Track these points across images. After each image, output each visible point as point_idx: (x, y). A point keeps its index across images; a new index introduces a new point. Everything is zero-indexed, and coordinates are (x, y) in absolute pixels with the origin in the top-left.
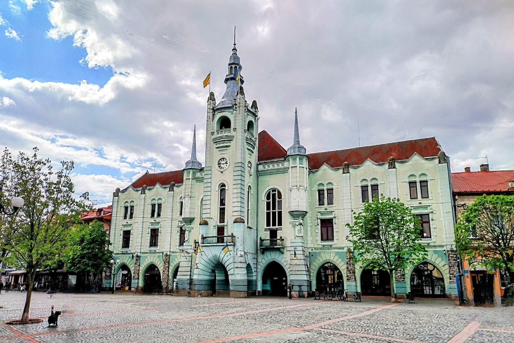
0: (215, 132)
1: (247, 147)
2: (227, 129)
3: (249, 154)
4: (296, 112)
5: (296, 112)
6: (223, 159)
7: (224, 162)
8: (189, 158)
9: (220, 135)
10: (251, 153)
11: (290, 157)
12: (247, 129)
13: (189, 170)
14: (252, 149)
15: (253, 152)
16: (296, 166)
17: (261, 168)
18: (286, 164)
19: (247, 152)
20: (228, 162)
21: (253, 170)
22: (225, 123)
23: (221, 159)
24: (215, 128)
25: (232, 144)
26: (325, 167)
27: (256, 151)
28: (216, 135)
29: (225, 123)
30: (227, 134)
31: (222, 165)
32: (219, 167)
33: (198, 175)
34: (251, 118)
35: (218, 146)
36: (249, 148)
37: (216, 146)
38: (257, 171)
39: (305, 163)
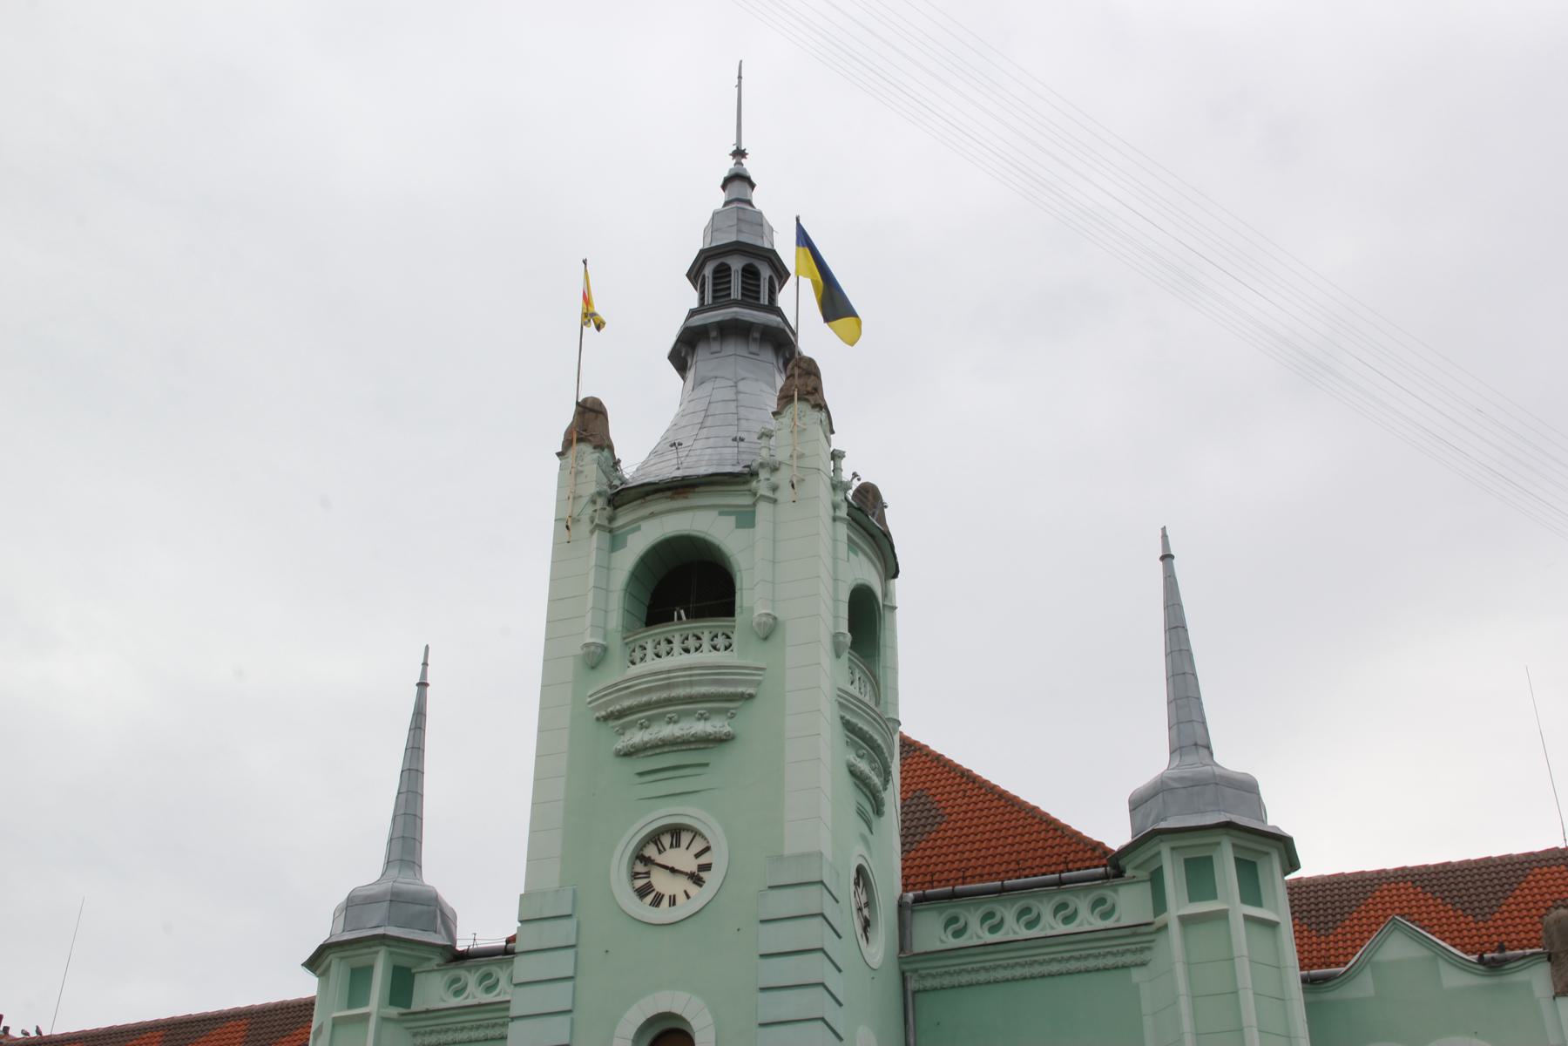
0: (616, 642)
1: (852, 757)
2: (706, 627)
3: (861, 813)
4: (1167, 557)
5: (1167, 557)
6: (676, 831)
7: (683, 858)
8: (367, 867)
9: (652, 664)
10: (868, 808)
11: (1165, 850)
12: (844, 627)
13: (360, 958)
14: (876, 781)
15: (878, 809)
16: (1222, 916)
17: (931, 932)
18: (1130, 904)
19: (850, 795)
20: (717, 858)
21: (880, 948)
22: (687, 586)
23: (654, 838)
24: (615, 619)
25: (745, 723)
26: (1397, 949)
27: (893, 797)
28: (617, 672)
29: (687, 586)
30: (706, 657)
31: (662, 882)
32: (642, 892)
33: (432, 991)
34: (866, 572)
35: (638, 737)
36: (863, 766)
37: (623, 742)
38: (907, 958)
39: (1278, 909)
